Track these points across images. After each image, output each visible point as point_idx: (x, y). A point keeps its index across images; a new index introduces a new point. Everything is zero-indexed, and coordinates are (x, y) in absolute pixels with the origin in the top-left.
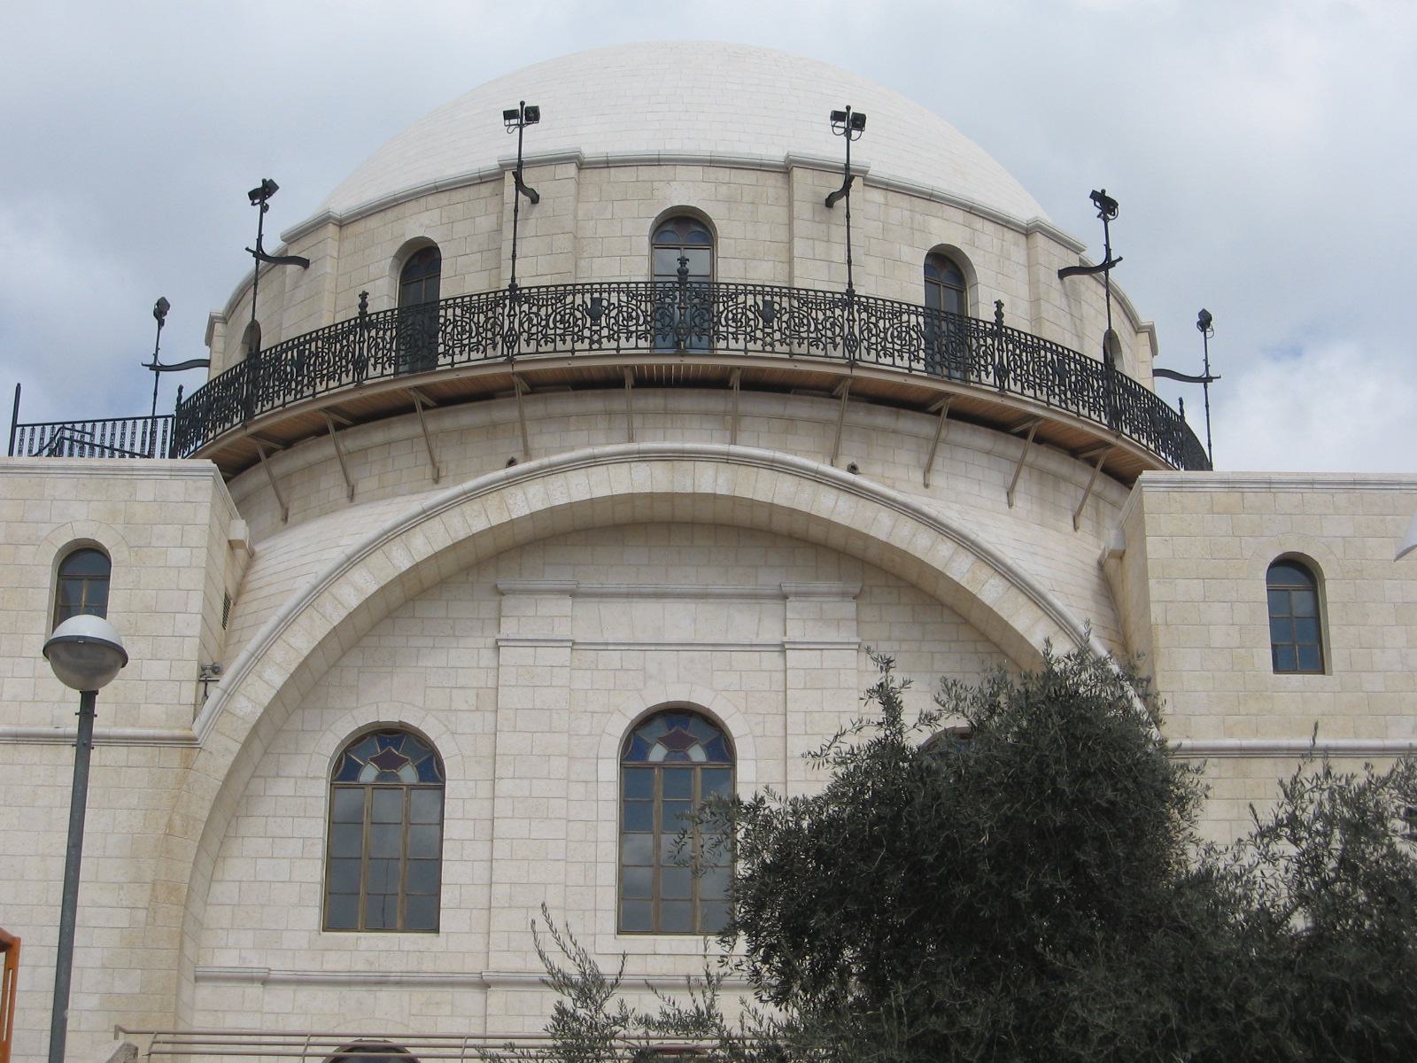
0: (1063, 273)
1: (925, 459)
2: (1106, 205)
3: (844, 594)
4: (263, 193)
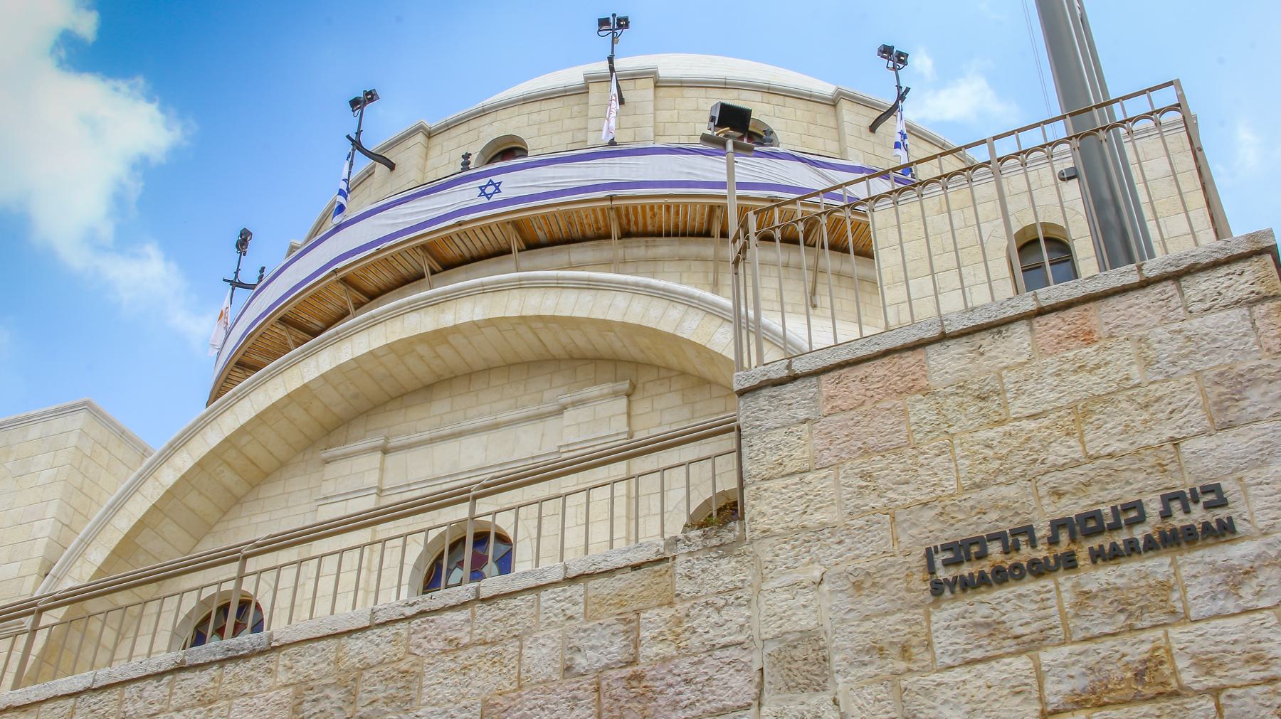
0: (873, 128)
1: (711, 276)
2: (894, 57)
3: (616, 394)
4: (243, 242)
